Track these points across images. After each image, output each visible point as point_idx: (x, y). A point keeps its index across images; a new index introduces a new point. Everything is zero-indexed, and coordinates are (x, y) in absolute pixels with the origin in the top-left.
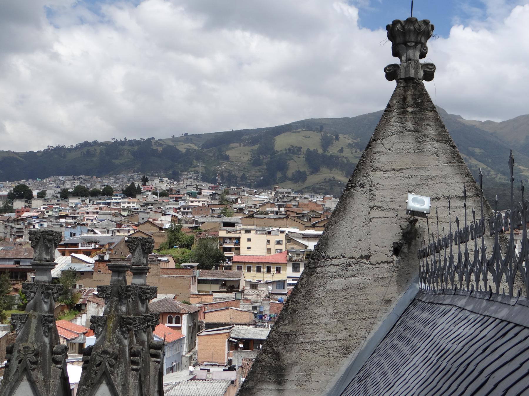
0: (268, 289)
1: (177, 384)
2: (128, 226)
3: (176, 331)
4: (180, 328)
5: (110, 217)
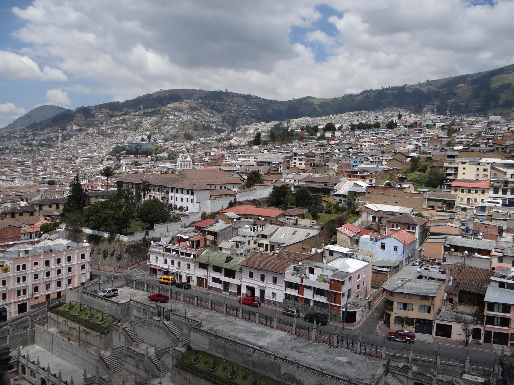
0: (474, 212)
1: (409, 280)
2: (388, 153)
3: (412, 235)
4: (414, 233)
5: (377, 148)
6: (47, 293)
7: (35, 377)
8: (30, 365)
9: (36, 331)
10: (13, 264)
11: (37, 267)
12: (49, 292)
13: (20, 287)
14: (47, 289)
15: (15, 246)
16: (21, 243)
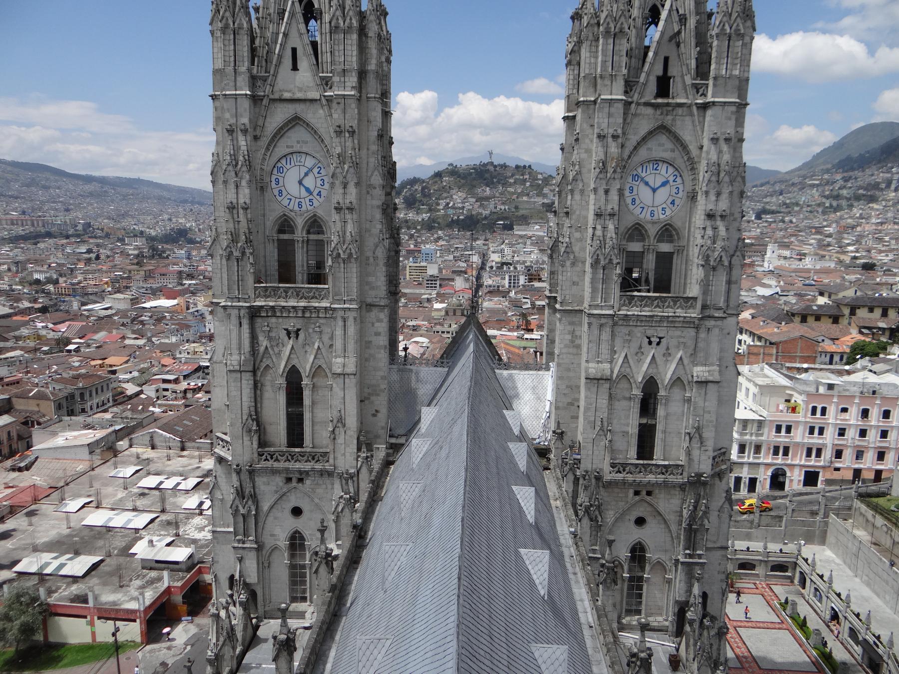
6: (856, 466)
7: (820, 601)
8: (815, 578)
9: (830, 526)
10: (807, 403)
11: (846, 416)
12: (861, 466)
13: (813, 444)
14: (857, 458)
15: (810, 372)
16: (821, 369)
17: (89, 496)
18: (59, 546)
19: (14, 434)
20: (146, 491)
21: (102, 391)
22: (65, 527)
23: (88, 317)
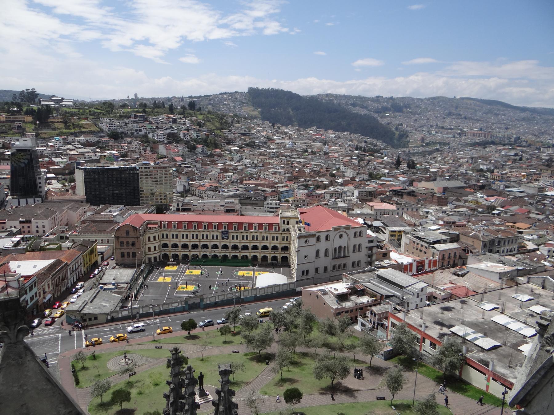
17: (497, 304)
18: (476, 326)
19: (458, 255)
20: (535, 314)
21: (512, 243)
22: (481, 317)
23: (508, 195)
